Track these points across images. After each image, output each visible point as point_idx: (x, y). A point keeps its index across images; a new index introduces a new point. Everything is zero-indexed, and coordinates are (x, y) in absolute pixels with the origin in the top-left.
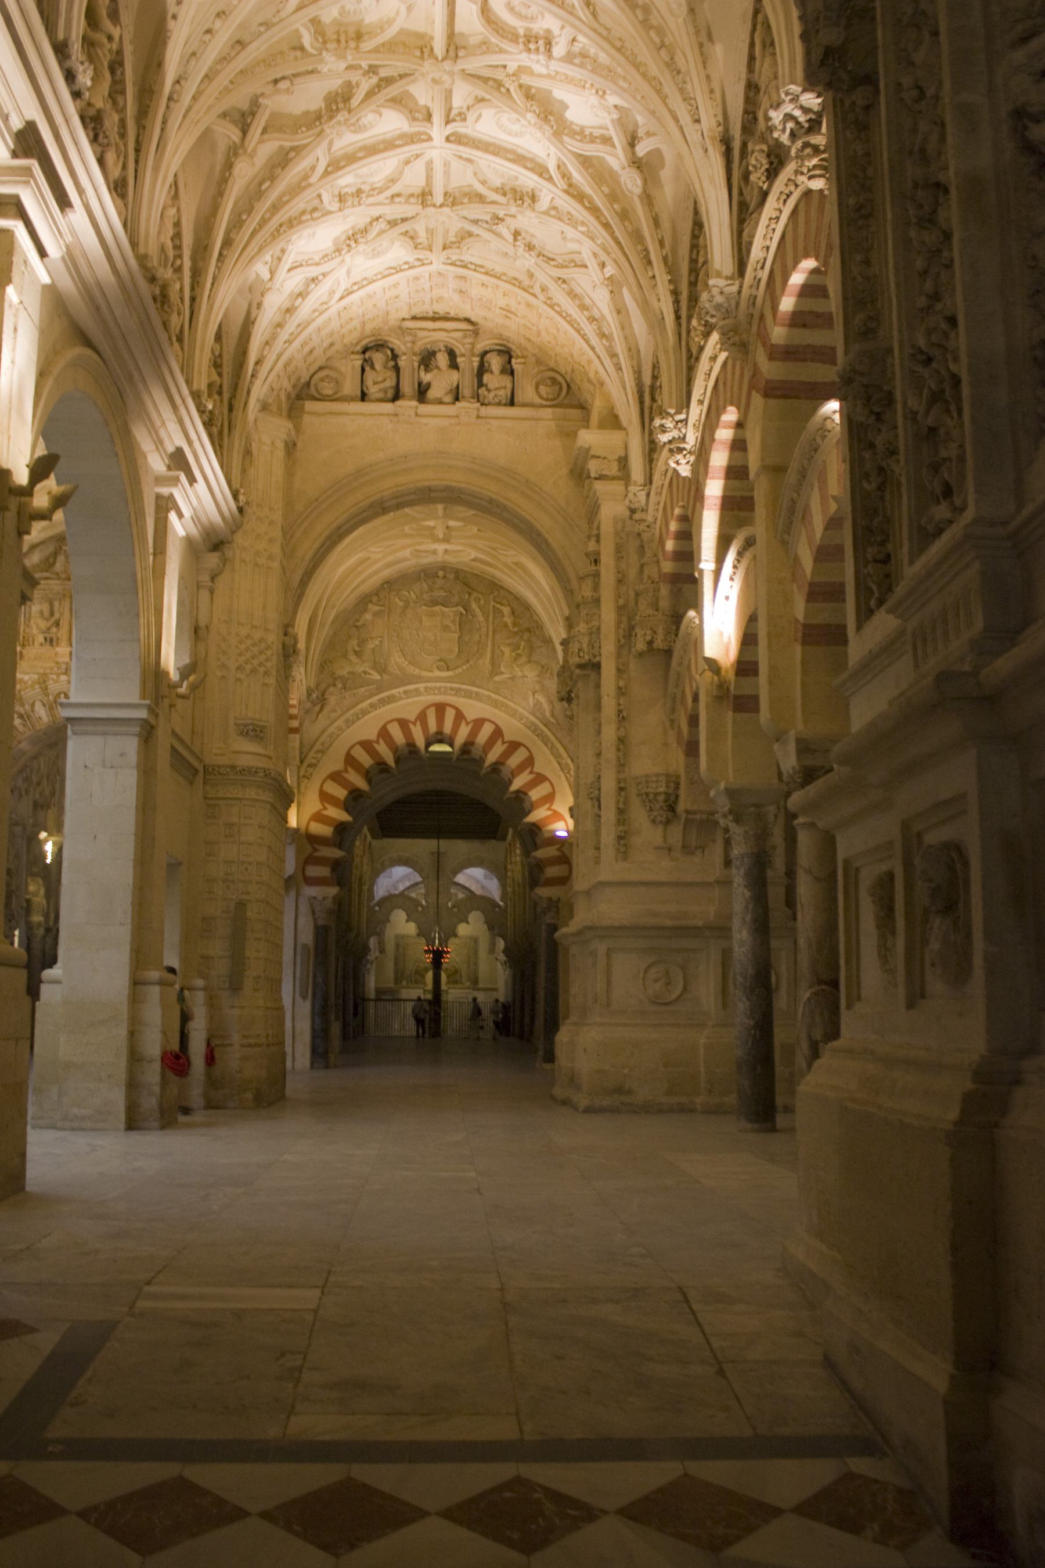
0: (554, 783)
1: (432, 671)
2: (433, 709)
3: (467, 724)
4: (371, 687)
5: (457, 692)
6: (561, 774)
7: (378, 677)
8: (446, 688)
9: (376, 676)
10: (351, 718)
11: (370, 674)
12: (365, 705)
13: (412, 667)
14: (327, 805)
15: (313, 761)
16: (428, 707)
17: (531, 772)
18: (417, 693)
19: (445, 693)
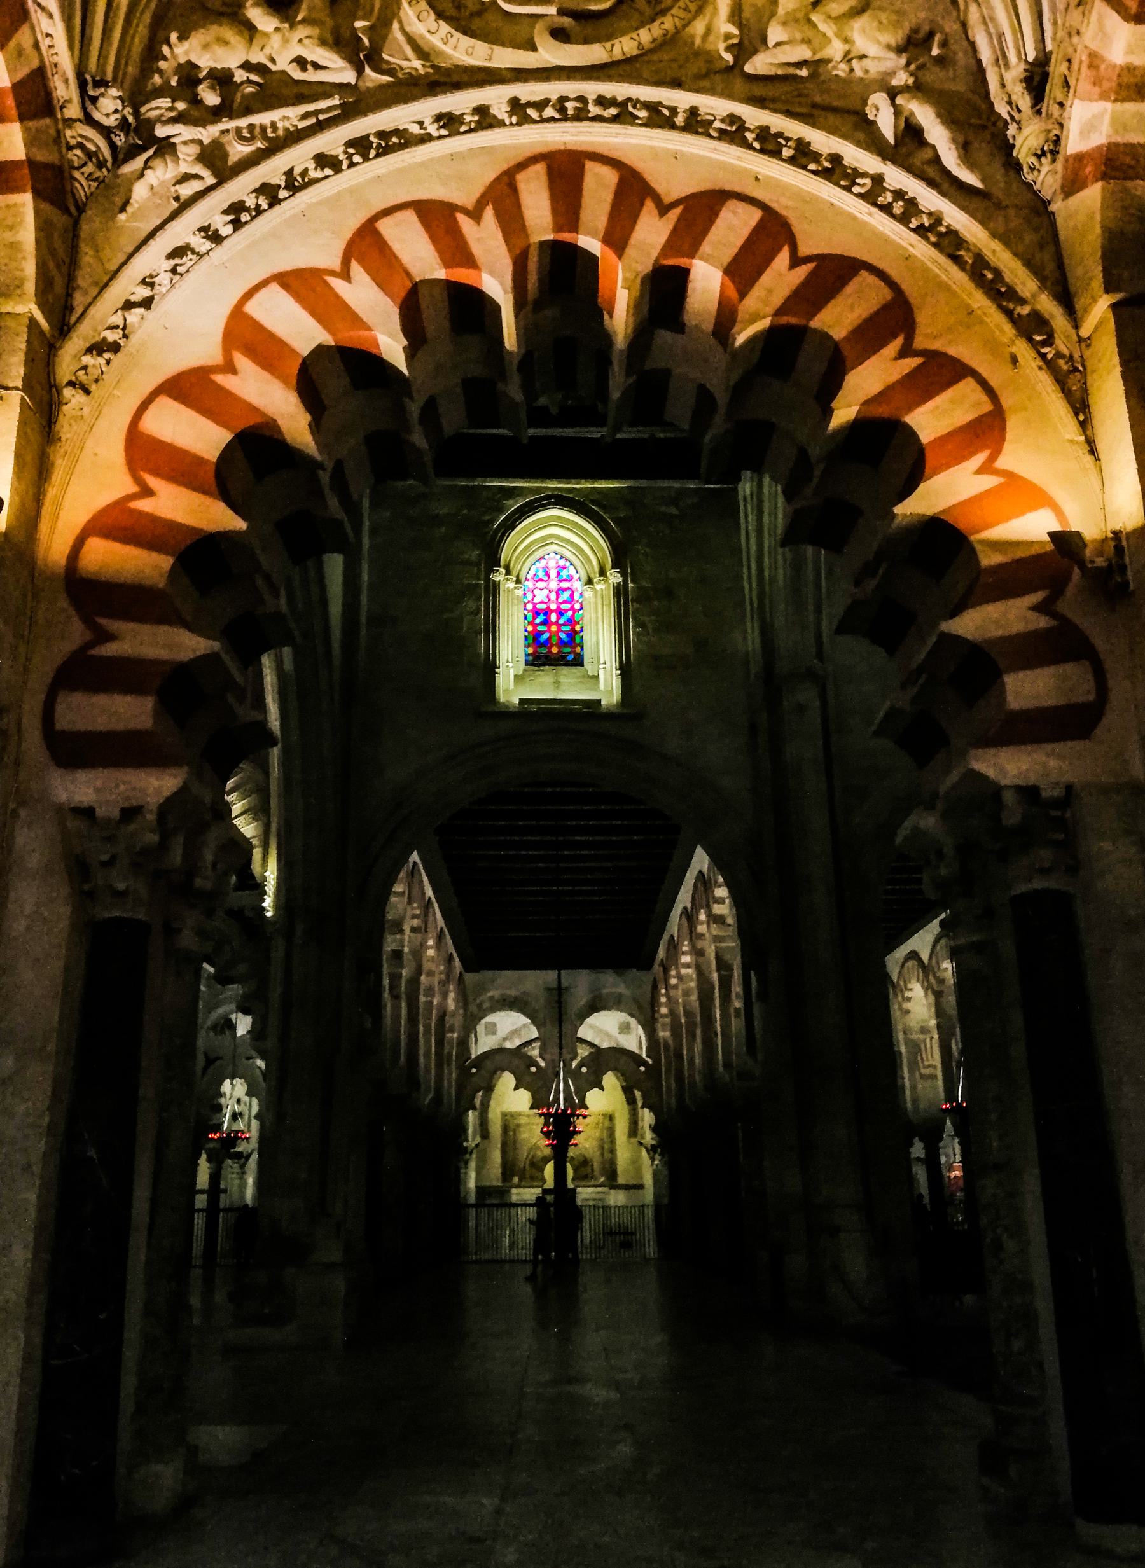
0: (993, 383)
1: (534, 49)
2: (540, 168)
3: (663, 209)
4: (322, 104)
5: (623, 113)
6: (1022, 349)
7: (348, 76)
8: (582, 99)
9: (339, 71)
10: (250, 202)
11: (317, 66)
12: (299, 156)
13: (466, 41)
14: (152, 481)
15: (112, 336)
16: (522, 166)
17: (906, 351)
18: (485, 119)
19: (581, 116)
